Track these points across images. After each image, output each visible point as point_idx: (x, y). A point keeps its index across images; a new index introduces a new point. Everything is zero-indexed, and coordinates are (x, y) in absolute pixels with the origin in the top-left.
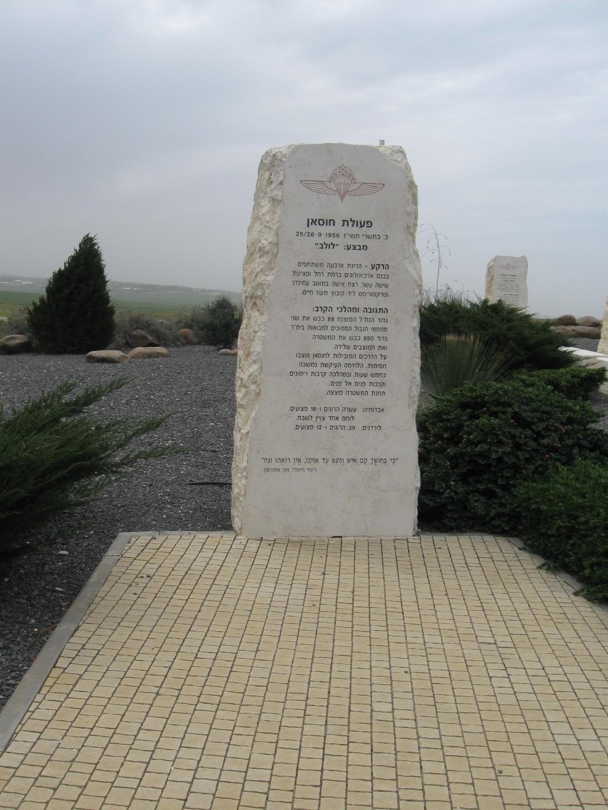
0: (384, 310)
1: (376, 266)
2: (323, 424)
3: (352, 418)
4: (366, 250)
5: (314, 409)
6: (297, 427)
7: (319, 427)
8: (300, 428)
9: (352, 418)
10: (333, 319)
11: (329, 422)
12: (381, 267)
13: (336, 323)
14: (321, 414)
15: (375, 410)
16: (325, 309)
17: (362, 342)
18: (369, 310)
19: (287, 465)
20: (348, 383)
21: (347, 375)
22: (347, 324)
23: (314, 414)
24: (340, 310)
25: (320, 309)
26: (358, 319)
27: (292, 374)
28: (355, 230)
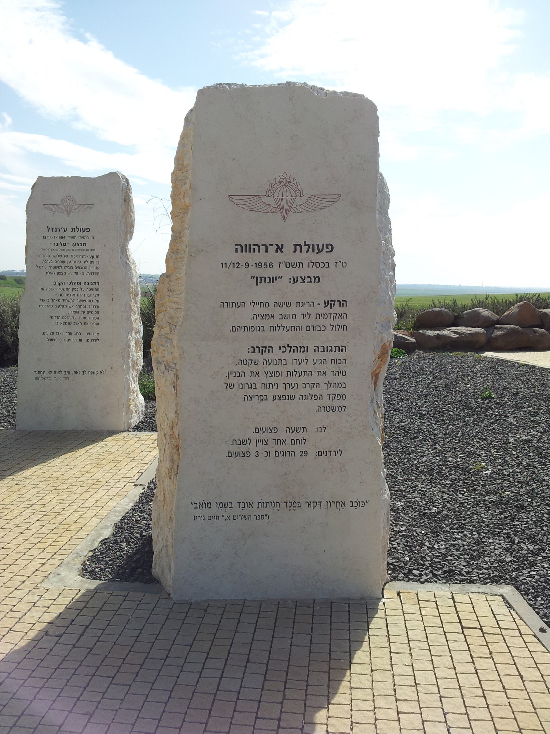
4: (317, 282)
24: (283, 349)
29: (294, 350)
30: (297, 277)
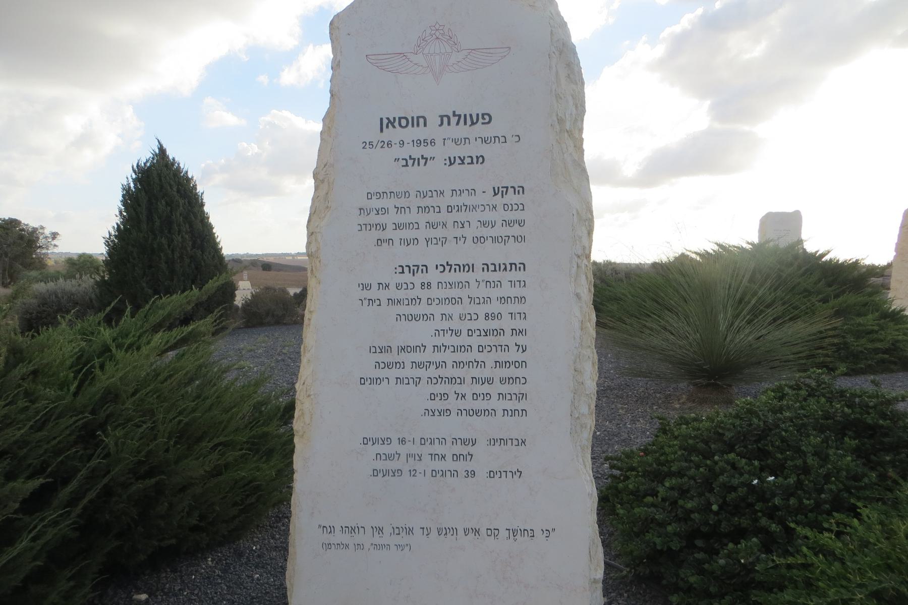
0: (518, 266)
1: (501, 190)
2: (420, 467)
3: (469, 457)
4: (481, 163)
5: (402, 441)
6: (375, 473)
7: (413, 473)
8: (381, 475)
9: (469, 457)
10: (429, 284)
11: (429, 464)
12: (511, 190)
13: (435, 293)
14: (416, 449)
15: (509, 442)
16: (414, 269)
17: (482, 324)
18: (492, 268)
19: (359, 538)
20: (460, 396)
21: (458, 381)
22: (454, 293)
23: (403, 450)
24: (441, 269)
25: (406, 269)
26: (473, 284)
27: (363, 381)
28: (462, 131)
29: (455, 269)
30: (455, 158)
